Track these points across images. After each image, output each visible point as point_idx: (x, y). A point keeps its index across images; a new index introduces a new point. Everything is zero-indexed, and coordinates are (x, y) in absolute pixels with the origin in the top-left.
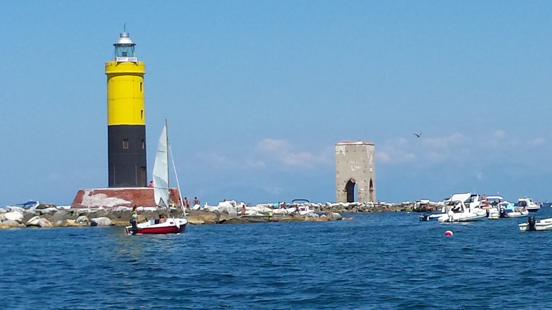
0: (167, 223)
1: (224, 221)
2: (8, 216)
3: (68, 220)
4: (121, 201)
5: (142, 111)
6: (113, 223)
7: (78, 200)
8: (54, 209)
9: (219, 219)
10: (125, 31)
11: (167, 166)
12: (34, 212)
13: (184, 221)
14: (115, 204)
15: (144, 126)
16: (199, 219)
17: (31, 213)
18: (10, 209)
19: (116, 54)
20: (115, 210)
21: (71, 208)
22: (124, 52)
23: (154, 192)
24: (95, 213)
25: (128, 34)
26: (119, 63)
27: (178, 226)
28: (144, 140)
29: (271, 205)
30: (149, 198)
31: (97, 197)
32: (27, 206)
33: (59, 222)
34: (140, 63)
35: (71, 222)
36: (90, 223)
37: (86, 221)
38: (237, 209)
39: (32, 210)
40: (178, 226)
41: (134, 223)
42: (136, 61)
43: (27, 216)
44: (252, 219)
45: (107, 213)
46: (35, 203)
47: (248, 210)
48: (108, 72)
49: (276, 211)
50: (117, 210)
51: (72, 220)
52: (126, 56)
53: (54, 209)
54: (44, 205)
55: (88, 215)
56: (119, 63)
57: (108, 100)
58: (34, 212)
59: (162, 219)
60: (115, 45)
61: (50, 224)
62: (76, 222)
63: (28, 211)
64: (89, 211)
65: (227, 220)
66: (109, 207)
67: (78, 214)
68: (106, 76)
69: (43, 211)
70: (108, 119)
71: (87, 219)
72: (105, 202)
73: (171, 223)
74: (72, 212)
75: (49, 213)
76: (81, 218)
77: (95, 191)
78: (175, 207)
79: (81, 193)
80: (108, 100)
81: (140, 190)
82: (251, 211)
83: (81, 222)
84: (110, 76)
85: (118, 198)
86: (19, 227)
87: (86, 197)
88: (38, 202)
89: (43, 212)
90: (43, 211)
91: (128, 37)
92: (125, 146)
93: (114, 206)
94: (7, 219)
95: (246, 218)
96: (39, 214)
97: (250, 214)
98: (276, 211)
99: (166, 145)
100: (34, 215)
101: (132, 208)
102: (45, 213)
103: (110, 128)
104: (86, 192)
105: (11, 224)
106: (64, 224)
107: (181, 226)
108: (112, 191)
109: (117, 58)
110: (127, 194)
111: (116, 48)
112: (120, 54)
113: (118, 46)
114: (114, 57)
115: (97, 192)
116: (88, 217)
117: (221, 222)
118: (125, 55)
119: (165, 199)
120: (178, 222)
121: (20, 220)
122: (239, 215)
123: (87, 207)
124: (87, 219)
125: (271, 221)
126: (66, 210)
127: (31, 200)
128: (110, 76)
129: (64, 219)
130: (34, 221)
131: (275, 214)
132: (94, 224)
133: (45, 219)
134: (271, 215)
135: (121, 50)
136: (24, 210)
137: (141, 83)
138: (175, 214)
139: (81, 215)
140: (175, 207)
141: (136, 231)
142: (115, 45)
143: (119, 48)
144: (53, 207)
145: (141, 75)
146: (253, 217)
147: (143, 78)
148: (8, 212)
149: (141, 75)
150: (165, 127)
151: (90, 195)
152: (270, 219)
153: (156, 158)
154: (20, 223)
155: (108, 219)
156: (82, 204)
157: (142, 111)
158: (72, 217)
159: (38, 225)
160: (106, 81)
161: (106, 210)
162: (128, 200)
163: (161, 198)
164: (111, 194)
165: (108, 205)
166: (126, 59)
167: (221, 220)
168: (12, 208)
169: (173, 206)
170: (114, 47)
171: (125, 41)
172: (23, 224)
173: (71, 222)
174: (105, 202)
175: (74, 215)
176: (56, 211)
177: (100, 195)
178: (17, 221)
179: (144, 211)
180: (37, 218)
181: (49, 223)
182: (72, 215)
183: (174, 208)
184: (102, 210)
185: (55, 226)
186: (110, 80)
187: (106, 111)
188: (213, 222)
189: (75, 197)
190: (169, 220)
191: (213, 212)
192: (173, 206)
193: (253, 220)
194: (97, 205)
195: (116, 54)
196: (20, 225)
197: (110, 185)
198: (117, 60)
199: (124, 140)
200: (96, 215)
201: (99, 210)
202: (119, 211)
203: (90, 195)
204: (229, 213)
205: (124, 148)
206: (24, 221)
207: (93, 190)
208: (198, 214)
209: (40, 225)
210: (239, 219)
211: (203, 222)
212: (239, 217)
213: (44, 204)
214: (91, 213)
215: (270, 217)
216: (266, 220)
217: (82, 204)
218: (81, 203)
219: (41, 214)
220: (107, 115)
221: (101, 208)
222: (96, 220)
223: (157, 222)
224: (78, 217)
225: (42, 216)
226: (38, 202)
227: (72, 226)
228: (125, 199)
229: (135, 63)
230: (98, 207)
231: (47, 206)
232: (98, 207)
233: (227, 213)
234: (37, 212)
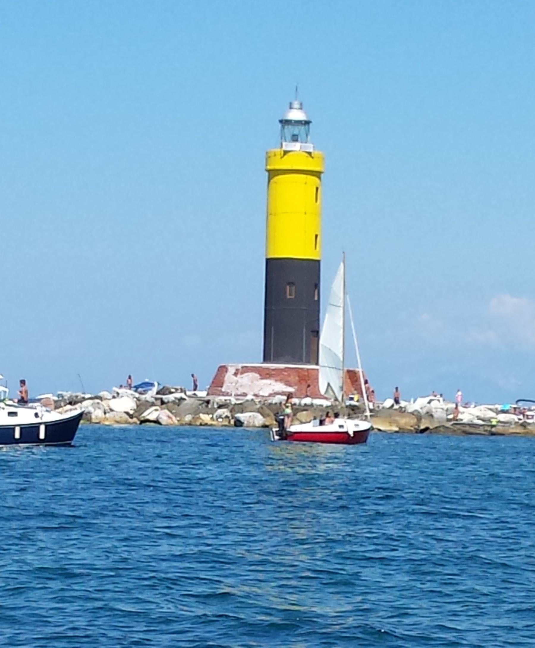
0: (332, 427)
1: (427, 429)
2: (115, 404)
3: (202, 416)
4: (280, 387)
5: (316, 236)
6: (267, 424)
7: (217, 383)
8: (183, 395)
9: (419, 426)
10: (296, 99)
11: (342, 330)
12: (153, 400)
13: (364, 426)
14: (271, 392)
15: (318, 262)
16: (391, 424)
17: (147, 401)
18: (118, 394)
19: (283, 137)
20: (270, 401)
21: (208, 395)
22: (294, 135)
23: (318, 372)
24: (241, 404)
25: (301, 104)
26: (286, 152)
27: (351, 433)
28: (317, 286)
29: (500, 407)
30: (308, 383)
31: (246, 378)
32: (140, 390)
33: (188, 418)
34: (315, 153)
35: (206, 418)
36: (232, 422)
37: (227, 417)
38: (447, 410)
39: (150, 395)
40: (351, 433)
41: (281, 423)
42: (311, 150)
43: (142, 406)
44: (467, 428)
45: (258, 406)
46: (152, 385)
47: (463, 413)
48: (269, 167)
49: (502, 417)
50: (274, 402)
51: (206, 416)
52: (297, 140)
53: (183, 395)
54: (168, 389)
55: (231, 407)
56: (286, 152)
57: (268, 214)
58: (153, 400)
59: (327, 419)
60: (281, 121)
61: (175, 420)
62: (212, 418)
63: (143, 397)
64: (234, 401)
65: (431, 427)
66: (263, 396)
67: (216, 406)
68: (267, 174)
69: (165, 398)
70: (267, 249)
71: (229, 414)
72: (257, 387)
73: (341, 426)
74: (208, 402)
75: (173, 402)
76: (220, 411)
77: (243, 367)
78: (358, 401)
79: (223, 369)
80: (268, 214)
81: (308, 369)
82: (468, 415)
83: (220, 420)
84: (273, 173)
85: (276, 381)
86: (129, 423)
87: (229, 376)
88: (156, 384)
89: (166, 401)
90: (165, 398)
91: (301, 108)
92: (290, 293)
93: (270, 395)
94: (112, 410)
95: (458, 426)
96: (159, 402)
97: (465, 421)
98: (502, 417)
99: (342, 295)
100: (153, 404)
101: (285, 398)
102: (168, 402)
103: (269, 261)
104: (229, 368)
105: (118, 419)
106: (195, 421)
107: (355, 432)
108: (268, 369)
109: (284, 144)
110: (289, 375)
111: (283, 127)
112: (289, 137)
113: (285, 122)
114: (280, 141)
115: (246, 370)
116: (231, 411)
117: (423, 431)
118: (295, 138)
119: (336, 387)
120: (351, 426)
121: (131, 412)
122: (449, 420)
123: (231, 395)
124: (229, 414)
125: (493, 434)
126: (200, 399)
127: (147, 380)
128: (273, 173)
129: (196, 413)
130: (151, 414)
131: (499, 422)
132: (239, 423)
133: (166, 411)
134: (494, 423)
135: (290, 130)
136: (137, 395)
137: (317, 189)
138: (354, 411)
139: (220, 407)
140: (358, 401)
141: (285, 436)
142: (281, 121)
143: (286, 127)
144: (181, 392)
145: (317, 174)
146: (469, 425)
147: (320, 178)
148: (114, 397)
149: (317, 174)
150: (342, 264)
151: (236, 374)
152: (493, 430)
153: (327, 315)
154: (131, 417)
155: (260, 417)
156: (223, 389)
157: (316, 236)
158: (207, 410)
159: (157, 422)
160: (266, 184)
161: (257, 400)
162: (290, 386)
163: (329, 385)
164: (265, 374)
165: (261, 393)
166: (296, 146)
167: (422, 427)
168: (120, 391)
169: (356, 399)
170: (280, 125)
171: (296, 115)
172: (135, 420)
173: (206, 418)
174: (257, 387)
175: (210, 406)
176: (184, 399)
177: (251, 375)
178: (127, 413)
179: (312, 405)
180: (156, 410)
181: (174, 418)
182: (207, 406)
183: (357, 404)
184: (252, 400)
185: (182, 425)
186: (272, 181)
187: (265, 234)
188: (411, 431)
189: (213, 376)
190: (338, 421)
191: (412, 413)
192: (356, 399)
193: (468, 431)
194: (245, 391)
195: (283, 137)
196: (130, 420)
197: (266, 358)
198: (284, 148)
199: (289, 284)
200: (242, 408)
201: (247, 401)
202: (276, 404)
203: (236, 374)
204: (435, 416)
205: (289, 297)
206: (136, 414)
207: (240, 366)
208: (390, 416)
209: (160, 420)
210: (448, 428)
211: (397, 429)
212: (449, 424)
213: (168, 386)
214: (235, 404)
215: (493, 426)
216: (490, 432)
217: (223, 389)
218: (222, 387)
219: (163, 403)
220: (265, 238)
221: (249, 397)
222: (241, 416)
223: (322, 423)
224: (216, 411)
225: (164, 406)
226: (156, 384)
227: (206, 424)
228: (286, 385)
229: (310, 153)
230: (245, 395)
231: (173, 390)
232: (245, 395)
233: (432, 416)
234: (156, 399)
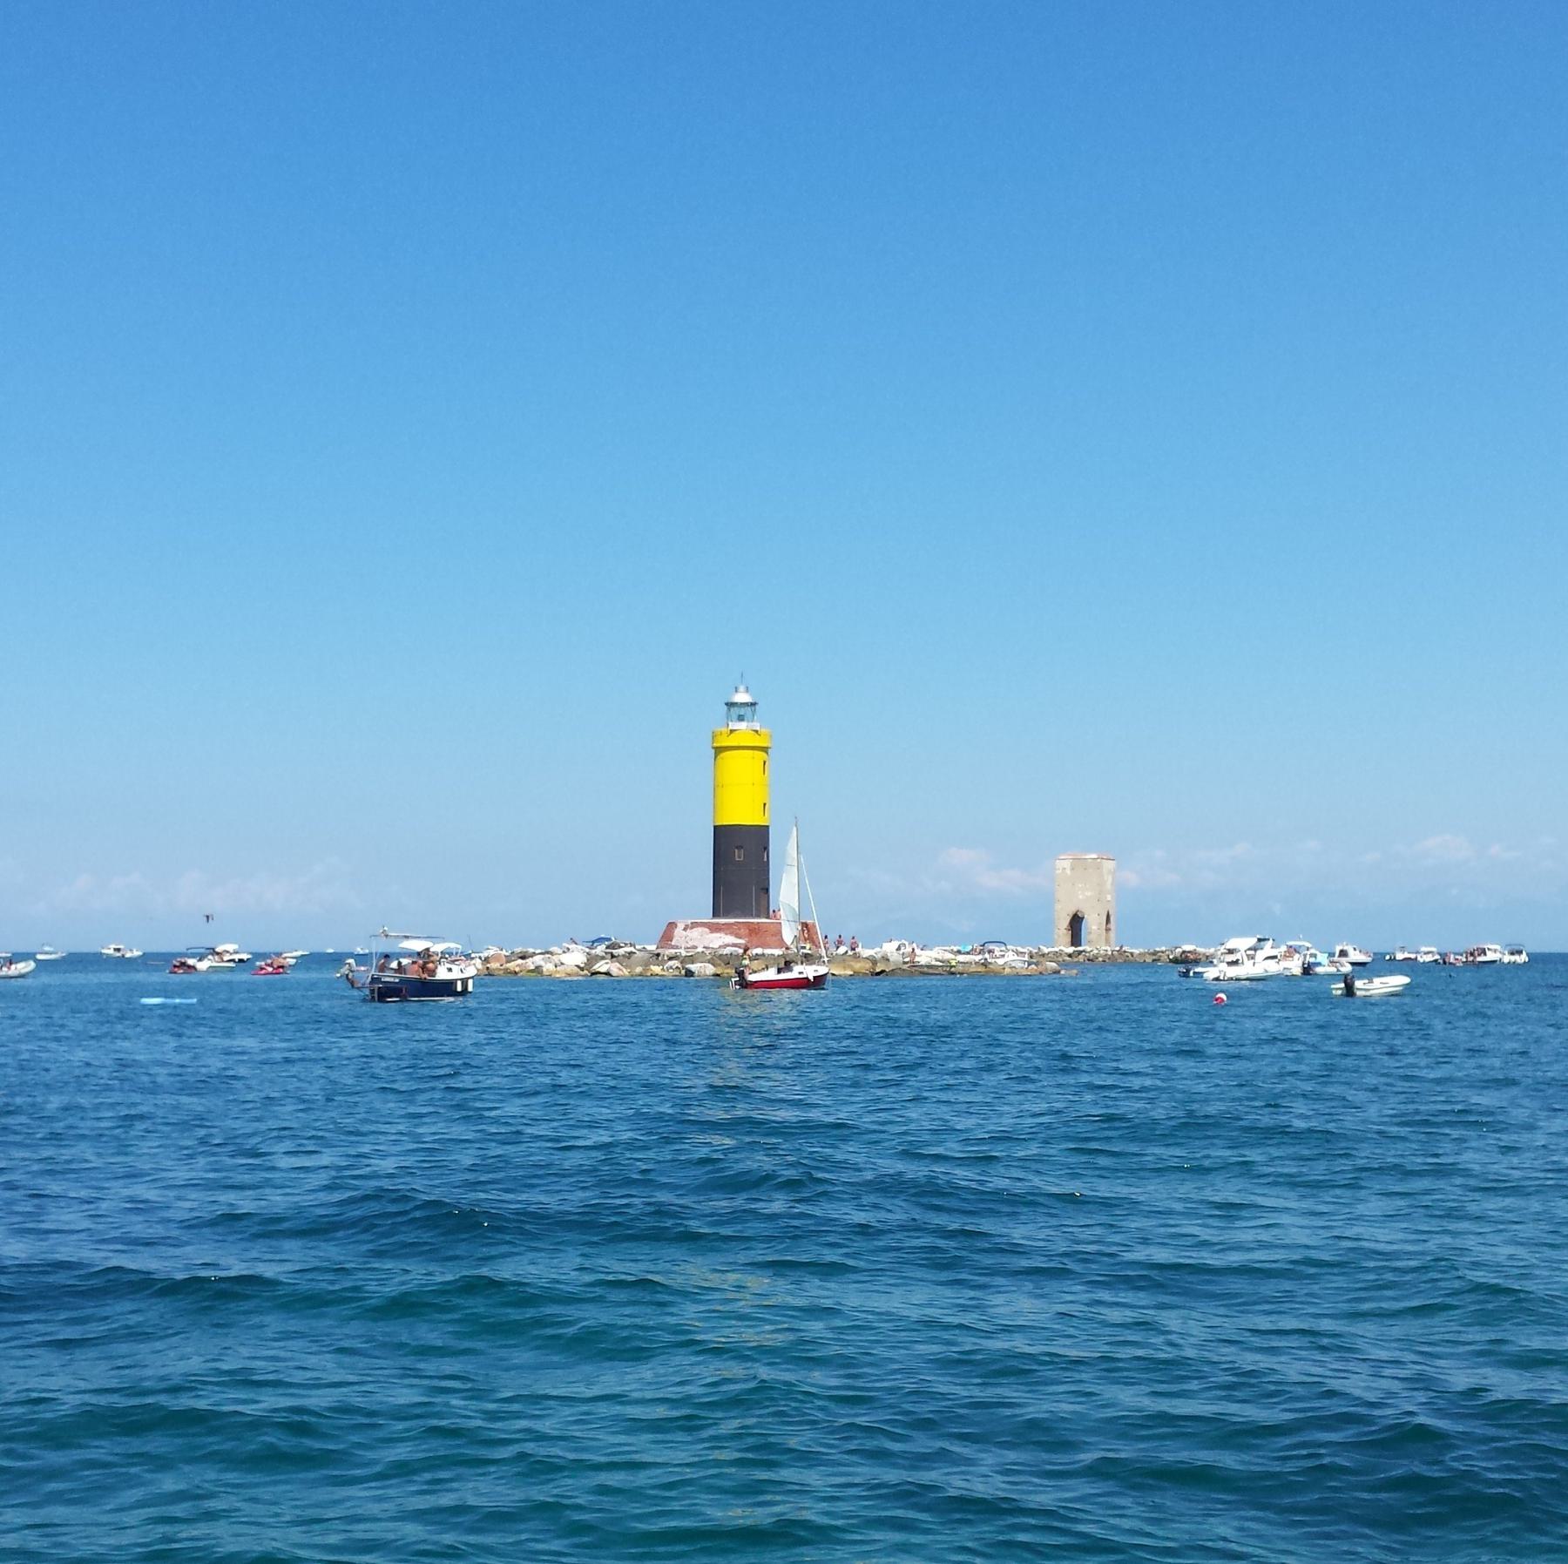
4: (731, 939)
7: (667, 937)
19: (729, 717)
31: (695, 933)
33: (639, 970)
35: (656, 969)
43: (592, 959)
72: (706, 940)
76: (671, 963)
79: (672, 925)
82: (924, 958)
84: (719, 750)
87: (679, 931)
90: (615, 952)
92: (739, 856)
112: (735, 717)
113: (730, 705)
115: (694, 925)
118: (741, 718)
126: (650, 952)
128: (719, 750)
129: (646, 965)
130: (602, 966)
132: (689, 973)
135: (735, 711)
139: (670, 959)
159: (607, 974)
166: (743, 725)
171: (742, 697)
173: (656, 969)
174: (706, 940)
193: (927, 971)
195: (729, 717)
197: (716, 914)
200: (692, 959)
216: (949, 971)
219: (613, 956)
221: (700, 949)
222: (692, 967)
